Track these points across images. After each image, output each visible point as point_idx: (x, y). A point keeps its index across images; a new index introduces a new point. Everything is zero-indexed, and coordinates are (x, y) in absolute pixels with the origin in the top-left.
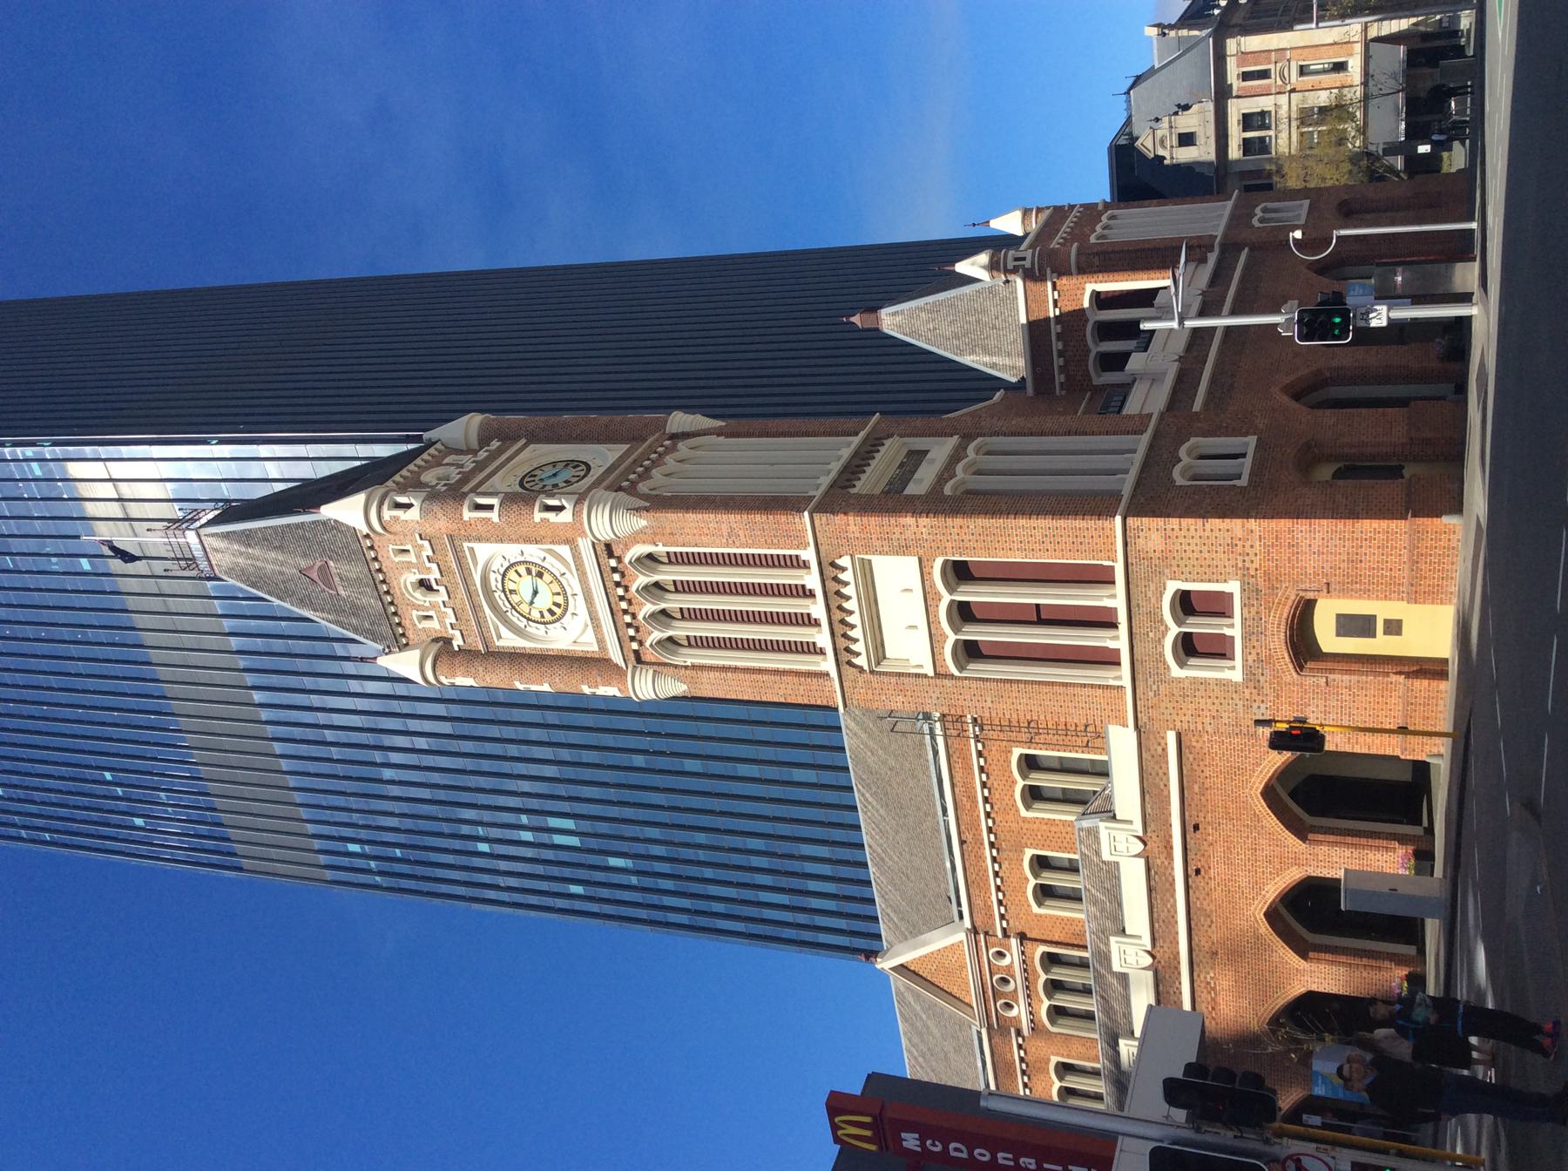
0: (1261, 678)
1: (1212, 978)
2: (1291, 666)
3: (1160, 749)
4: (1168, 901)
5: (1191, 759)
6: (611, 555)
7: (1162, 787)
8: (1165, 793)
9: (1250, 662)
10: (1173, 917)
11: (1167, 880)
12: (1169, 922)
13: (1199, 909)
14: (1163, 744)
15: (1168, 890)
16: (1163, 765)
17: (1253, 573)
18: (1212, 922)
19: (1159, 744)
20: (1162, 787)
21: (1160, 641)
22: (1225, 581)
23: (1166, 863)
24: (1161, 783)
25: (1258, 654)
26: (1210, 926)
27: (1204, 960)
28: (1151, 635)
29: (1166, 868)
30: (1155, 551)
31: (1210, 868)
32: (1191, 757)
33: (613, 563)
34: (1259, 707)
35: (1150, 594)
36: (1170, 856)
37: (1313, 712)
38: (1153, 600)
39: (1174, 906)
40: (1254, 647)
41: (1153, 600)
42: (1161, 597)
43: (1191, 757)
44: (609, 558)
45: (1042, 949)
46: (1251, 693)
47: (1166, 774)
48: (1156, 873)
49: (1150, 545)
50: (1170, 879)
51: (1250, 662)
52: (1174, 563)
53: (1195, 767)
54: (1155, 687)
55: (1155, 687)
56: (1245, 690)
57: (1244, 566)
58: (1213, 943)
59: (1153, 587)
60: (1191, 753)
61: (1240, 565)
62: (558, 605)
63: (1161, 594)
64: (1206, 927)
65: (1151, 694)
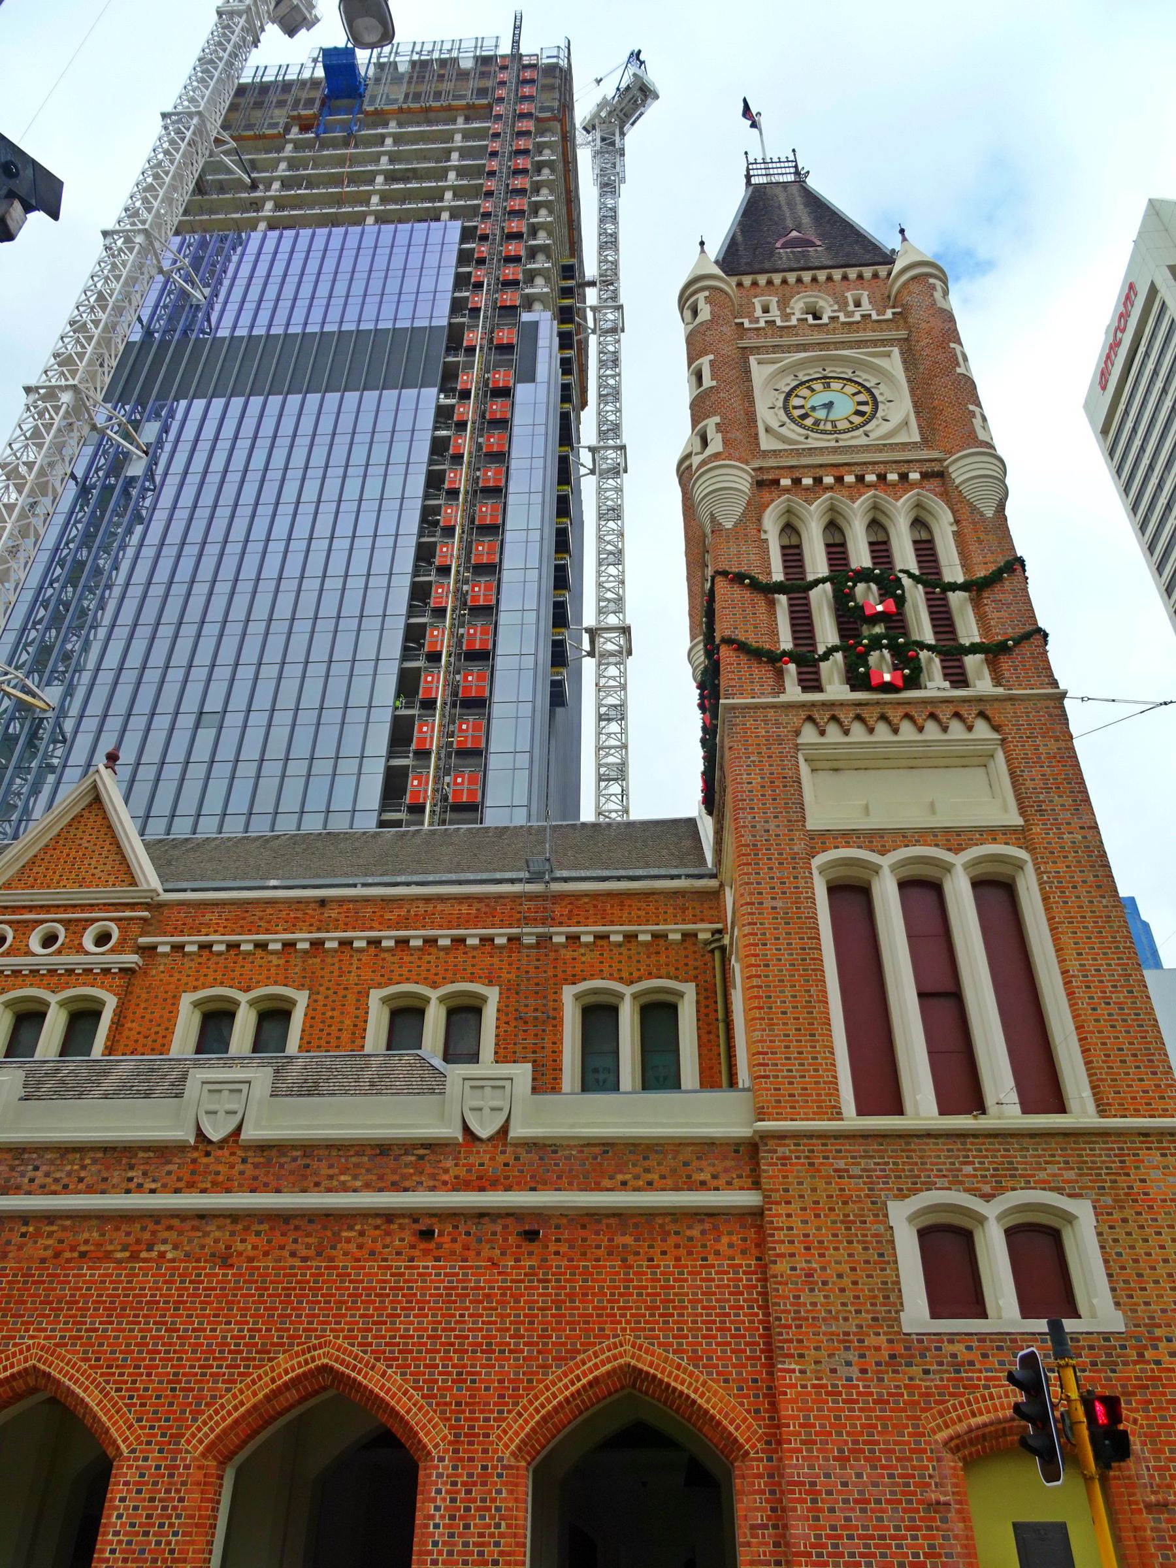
0: (916, 1370)
1: (162, 1255)
2: (960, 1428)
3: (703, 1176)
4: (355, 1177)
5: (688, 1233)
6: (925, 476)
7: (620, 1177)
8: (606, 1183)
9: (948, 1348)
10: (317, 1184)
11: (405, 1177)
12: (305, 1177)
13: (337, 1234)
14: (715, 1183)
15: (381, 1178)
16: (669, 1181)
17: (1148, 1355)
18: (305, 1259)
19: (714, 1177)
20: (620, 1177)
21: (956, 1182)
22: (1117, 1304)
23: (446, 1177)
24: (628, 1177)
25: (971, 1363)
26: (293, 1254)
27: (209, 1241)
28: (968, 1169)
29: (434, 1177)
30: (1143, 1181)
31: (437, 1259)
32: (695, 1233)
33: (914, 476)
34: (849, 1364)
35: (1053, 1169)
36: (462, 1185)
37: (859, 1475)
38: (1042, 1175)
39: (345, 1188)
40: (985, 1356)
41: (1042, 1175)
42: (1052, 1189)
43: (695, 1233)
44: (921, 473)
45: (111, 1003)
46: (878, 1349)
47: (650, 1186)
48: (421, 1157)
49: (1155, 1174)
50: (407, 1184)
51: (948, 1348)
52: (1129, 1213)
53: (672, 1240)
54: (855, 1170)
55: (855, 1170)
56: (883, 1338)
57: (1159, 1339)
58: (251, 1260)
59: (1070, 1175)
60: (703, 1232)
61: (1158, 1332)
62: (866, 403)
63: (1059, 1190)
64: (291, 1246)
65: (841, 1164)
